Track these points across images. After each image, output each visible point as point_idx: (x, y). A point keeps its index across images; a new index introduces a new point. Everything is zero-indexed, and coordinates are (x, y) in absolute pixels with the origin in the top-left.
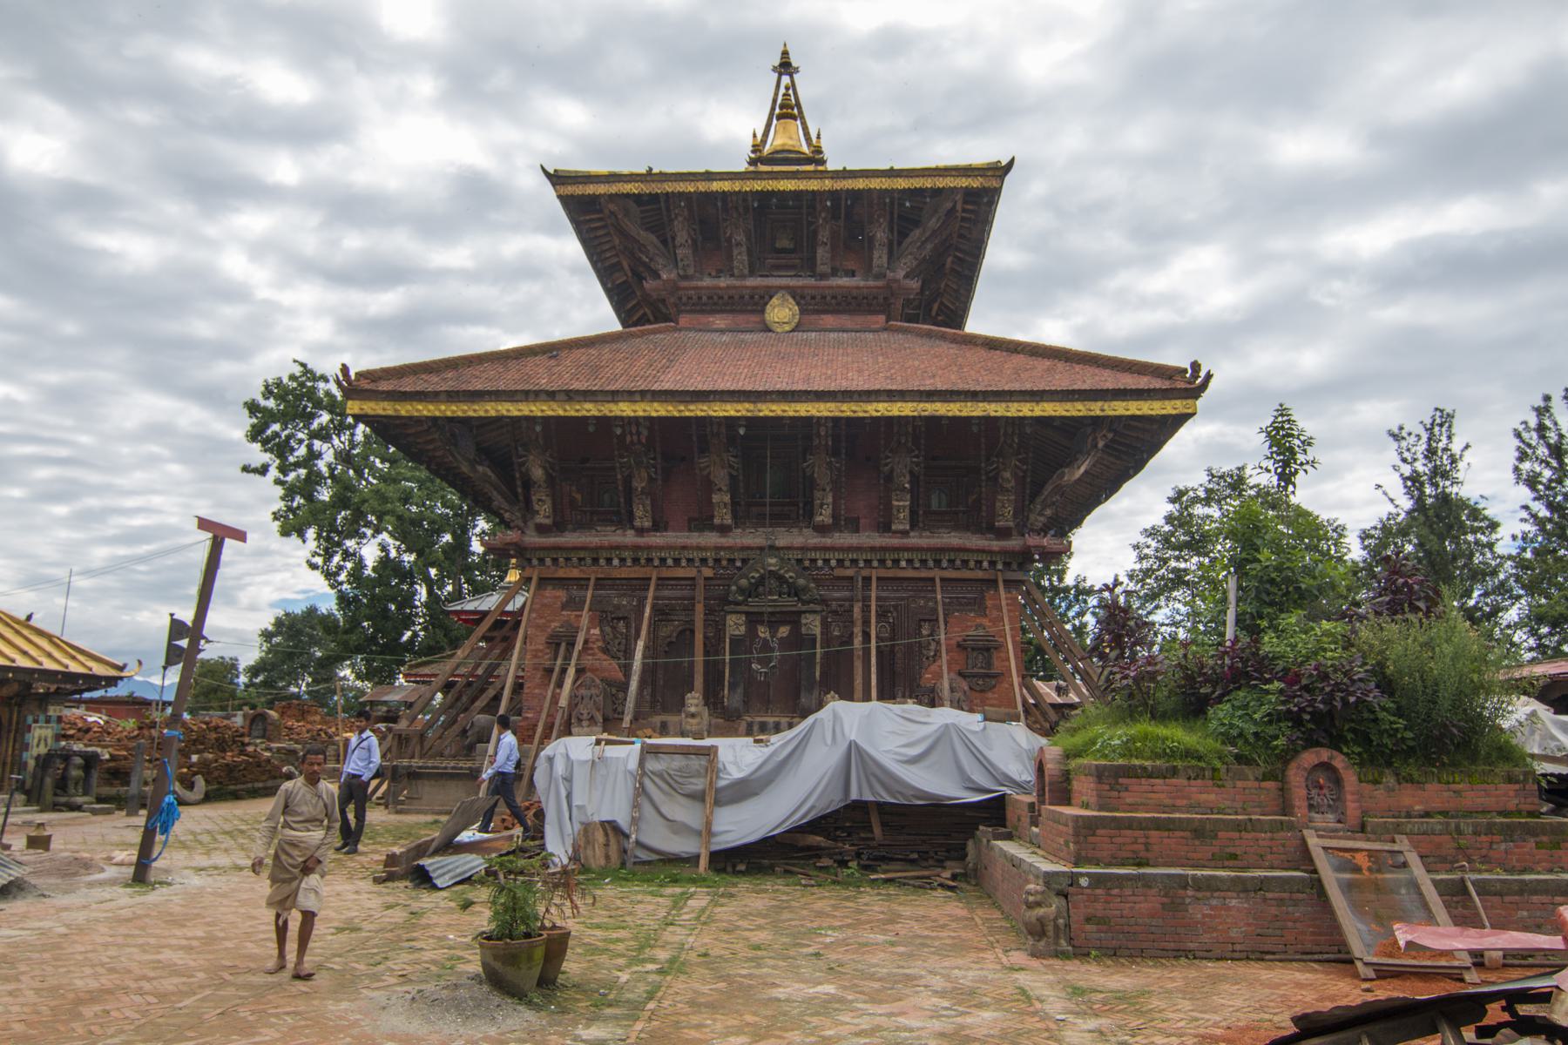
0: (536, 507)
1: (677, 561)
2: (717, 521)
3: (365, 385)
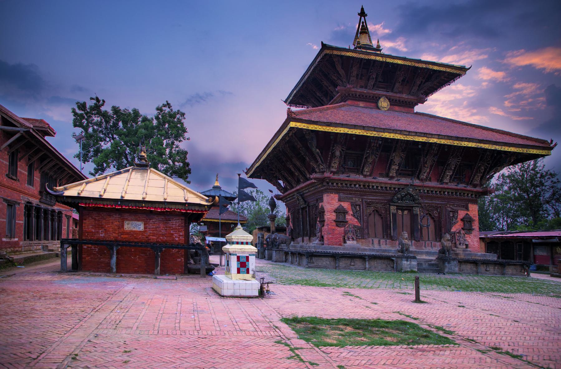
1: (377, 187)
2: (391, 175)
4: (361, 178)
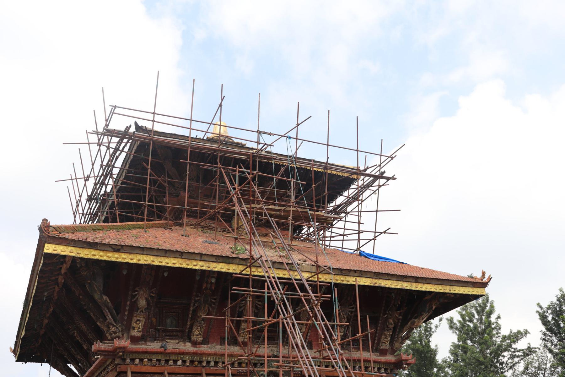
0: (134, 325)
3: (56, 234)
4: (188, 347)
